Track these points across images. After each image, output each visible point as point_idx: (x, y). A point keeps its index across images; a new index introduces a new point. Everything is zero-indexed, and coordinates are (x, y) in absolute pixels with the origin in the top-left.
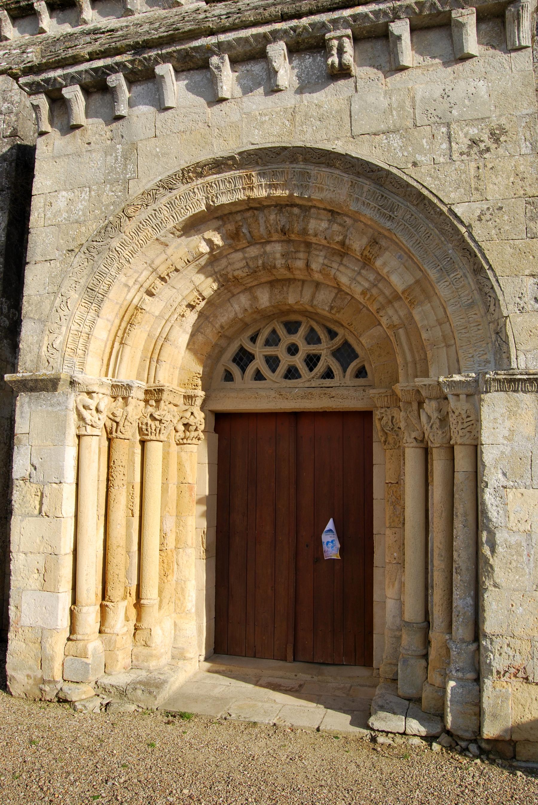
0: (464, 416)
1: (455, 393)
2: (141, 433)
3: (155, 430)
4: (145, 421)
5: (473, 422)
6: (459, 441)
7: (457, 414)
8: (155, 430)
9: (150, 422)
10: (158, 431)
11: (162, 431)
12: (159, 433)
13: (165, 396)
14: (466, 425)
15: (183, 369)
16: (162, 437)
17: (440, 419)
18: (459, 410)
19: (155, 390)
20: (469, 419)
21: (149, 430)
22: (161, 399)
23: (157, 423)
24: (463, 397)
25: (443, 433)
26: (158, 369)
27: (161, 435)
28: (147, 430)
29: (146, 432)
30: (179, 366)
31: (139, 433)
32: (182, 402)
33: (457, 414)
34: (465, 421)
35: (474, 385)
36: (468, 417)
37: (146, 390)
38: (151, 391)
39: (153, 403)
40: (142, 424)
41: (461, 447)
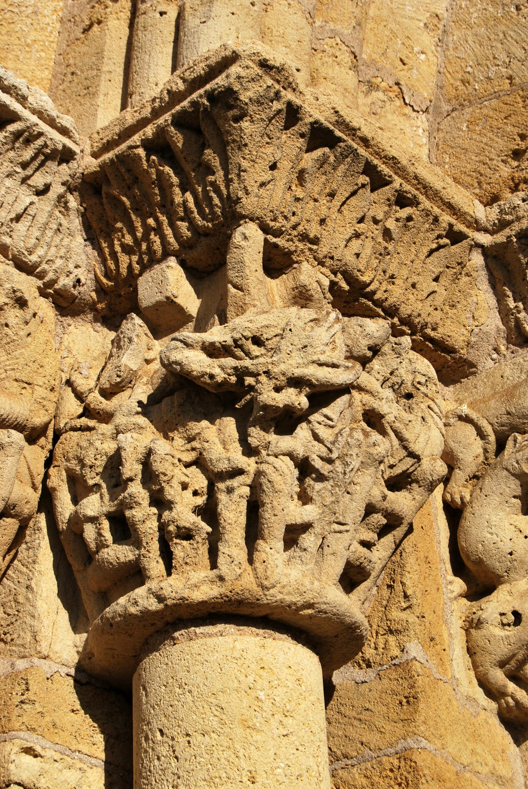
2: (87, 583)
3: (209, 512)
4: (100, 444)
8: (209, 512)
9: (139, 438)
10: (233, 513)
11: (284, 508)
12: (254, 532)
13: (266, 173)
15: (460, 104)
16: (297, 577)
19: (159, 146)
21: (144, 516)
22: (233, 216)
23: (219, 438)
26: (191, 22)
27: (272, 549)
28: (123, 528)
29: (118, 553)
30: (423, 76)
31: (70, 594)
32: (492, 322)
37: (90, 188)
38: (126, 161)
39: (172, 282)
40: (79, 488)
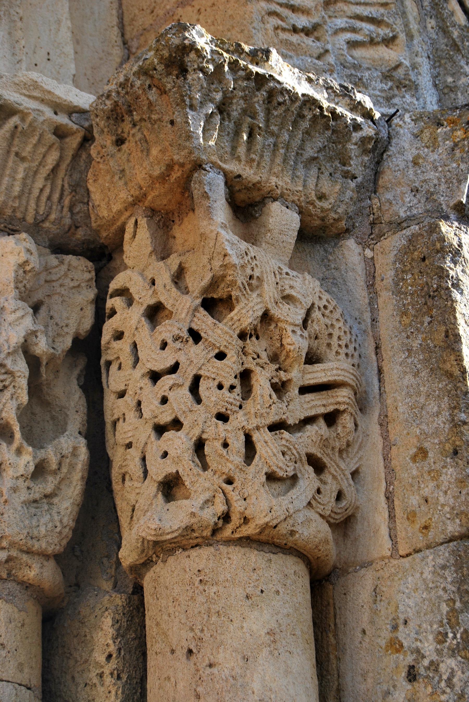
0: (297, 343)
1: (249, 174)
5: (343, 396)
6: (262, 506)
7: (246, 312)
14: (300, 407)
17: (33, 362)
18: (270, 291)
20: (318, 374)
24: (282, 220)
25: (40, 470)
33: (246, 312)
34: (298, 375)
35: (358, 164)
36: (312, 359)
41: (255, 557)
